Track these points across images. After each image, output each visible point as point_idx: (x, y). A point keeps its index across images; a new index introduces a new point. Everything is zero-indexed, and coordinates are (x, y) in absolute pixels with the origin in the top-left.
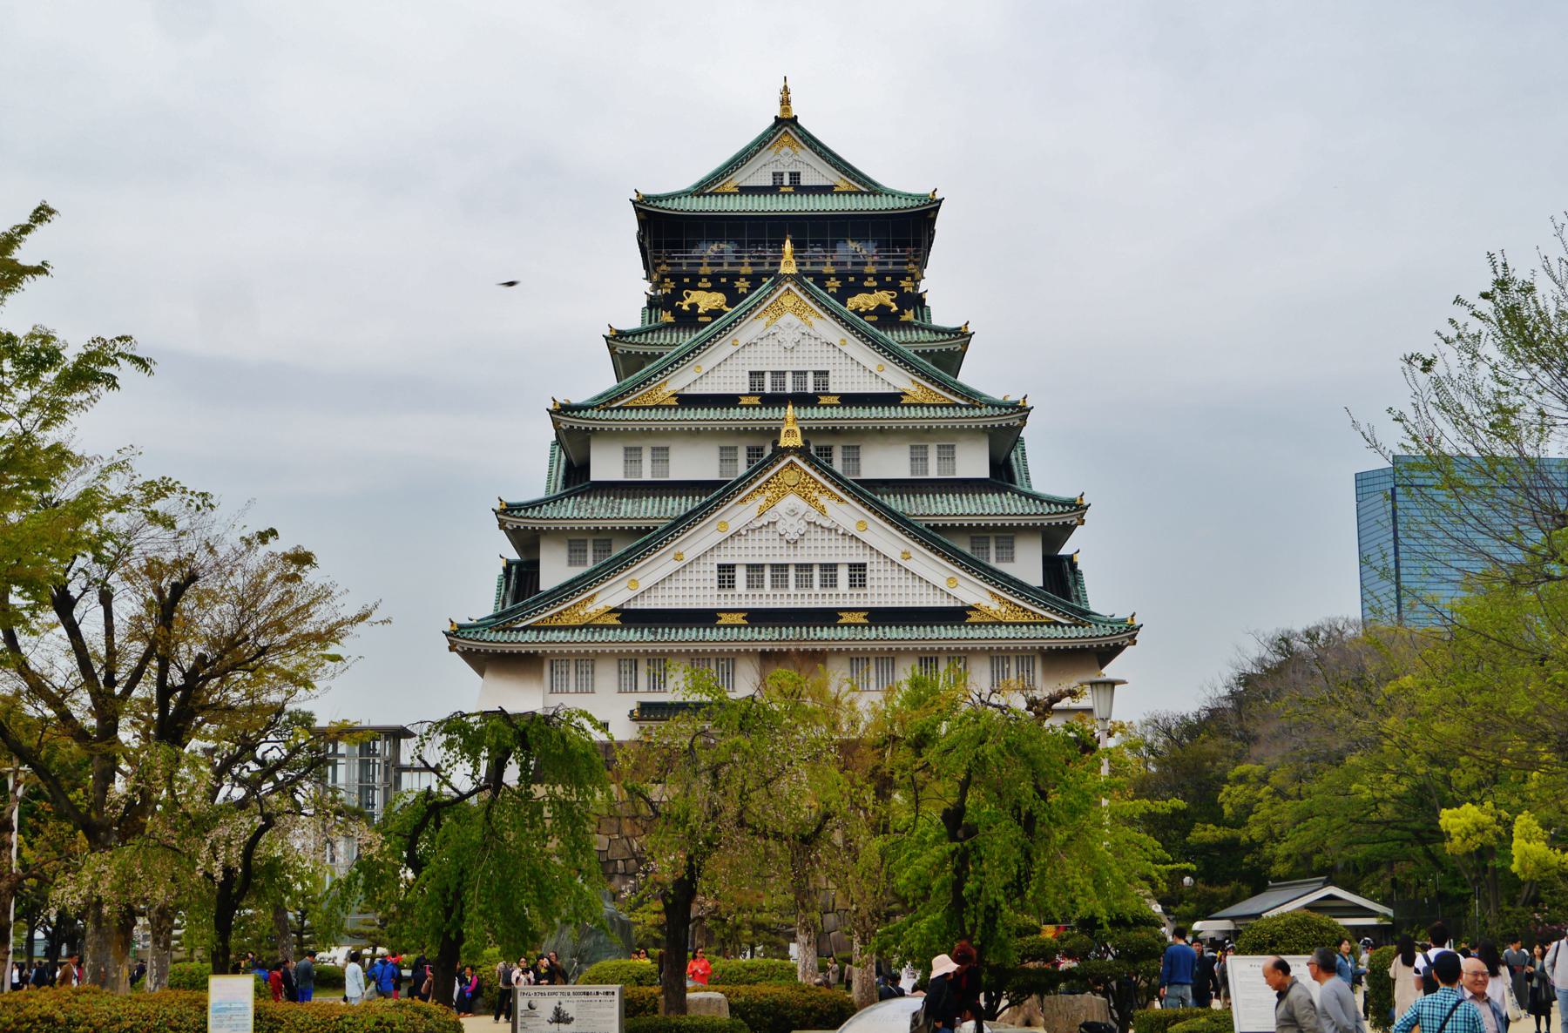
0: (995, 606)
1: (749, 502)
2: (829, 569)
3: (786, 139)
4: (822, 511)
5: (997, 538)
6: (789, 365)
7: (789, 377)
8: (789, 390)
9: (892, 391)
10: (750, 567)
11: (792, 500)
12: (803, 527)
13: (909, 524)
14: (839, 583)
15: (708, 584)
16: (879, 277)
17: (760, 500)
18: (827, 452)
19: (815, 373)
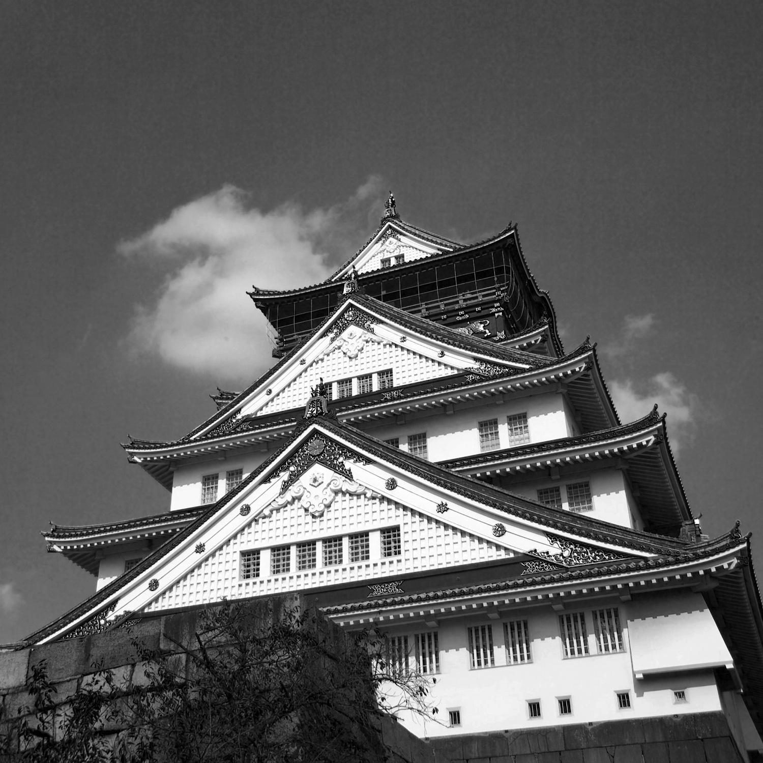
0: (555, 550)
1: (273, 481)
2: (360, 538)
3: (389, 232)
4: (348, 475)
5: (569, 488)
6: (352, 370)
7: (355, 382)
8: (355, 392)
9: (456, 372)
10: (274, 549)
11: (317, 470)
12: (329, 496)
13: (448, 475)
14: (371, 554)
15: (229, 575)
16: (468, 309)
17: (284, 476)
18: (396, 442)
19: (380, 374)
